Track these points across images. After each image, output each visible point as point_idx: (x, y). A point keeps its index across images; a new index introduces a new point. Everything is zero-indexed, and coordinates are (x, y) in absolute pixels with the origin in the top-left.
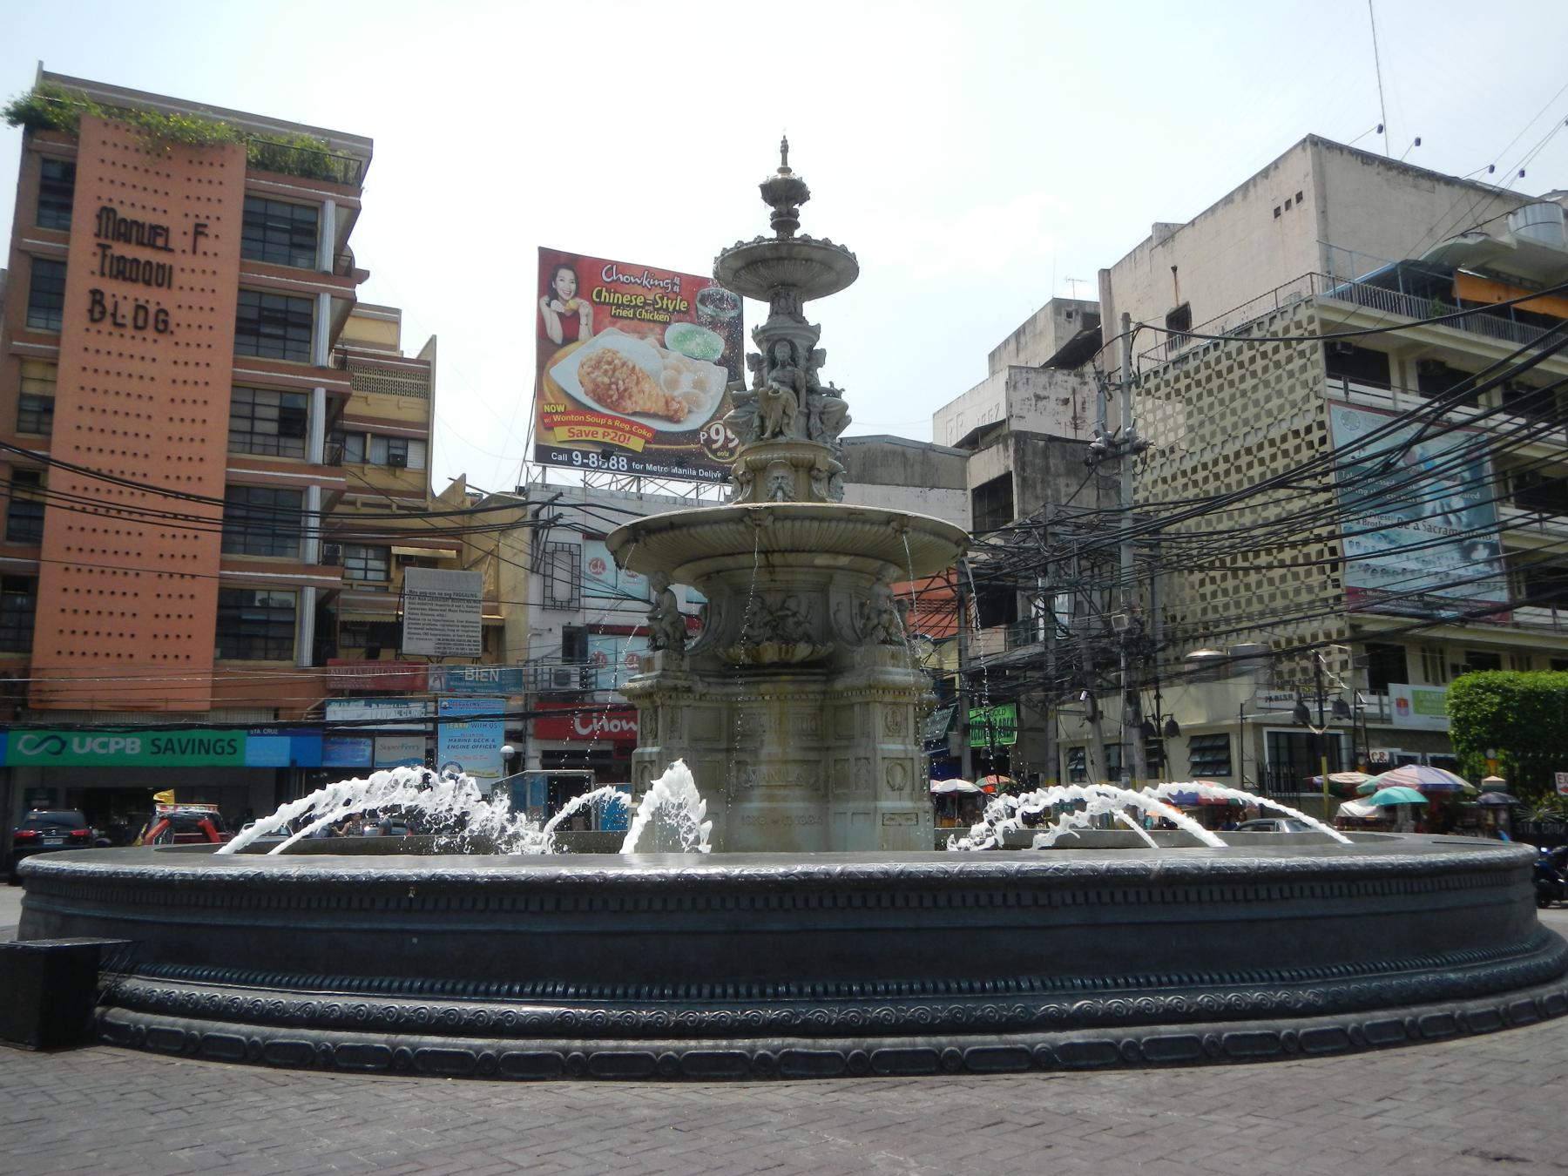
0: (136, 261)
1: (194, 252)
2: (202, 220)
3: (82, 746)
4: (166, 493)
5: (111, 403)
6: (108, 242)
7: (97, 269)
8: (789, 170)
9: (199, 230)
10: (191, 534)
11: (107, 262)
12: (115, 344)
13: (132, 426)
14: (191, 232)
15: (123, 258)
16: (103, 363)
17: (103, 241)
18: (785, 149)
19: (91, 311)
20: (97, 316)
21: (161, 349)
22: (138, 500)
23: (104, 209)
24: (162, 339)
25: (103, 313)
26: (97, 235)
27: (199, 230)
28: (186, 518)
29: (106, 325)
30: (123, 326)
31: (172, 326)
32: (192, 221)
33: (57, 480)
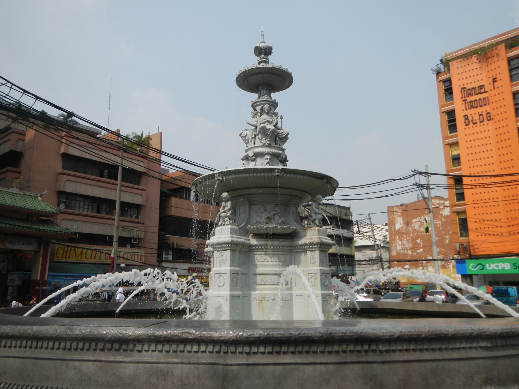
0: (476, 100)
1: (494, 89)
2: (494, 77)
3: (490, 267)
4: (502, 175)
5: (477, 149)
6: (466, 98)
7: (464, 109)
9: (495, 80)
10: (514, 187)
11: (467, 105)
12: (475, 130)
13: (486, 155)
14: (492, 82)
15: (471, 101)
16: (472, 137)
17: (464, 99)
19: (465, 122)
20: (467, 123)
21: (489, 126)
22: (493, 180)
23: (462, 88)
24: (490, 122)
25: (469, 122)
26: (462, 98)
27: (495, 80)
28: (511, 182)
29: (471, 124)
30: (476, 123)
31: (492, 117)
32: (491, 78)
33: (466, 180)
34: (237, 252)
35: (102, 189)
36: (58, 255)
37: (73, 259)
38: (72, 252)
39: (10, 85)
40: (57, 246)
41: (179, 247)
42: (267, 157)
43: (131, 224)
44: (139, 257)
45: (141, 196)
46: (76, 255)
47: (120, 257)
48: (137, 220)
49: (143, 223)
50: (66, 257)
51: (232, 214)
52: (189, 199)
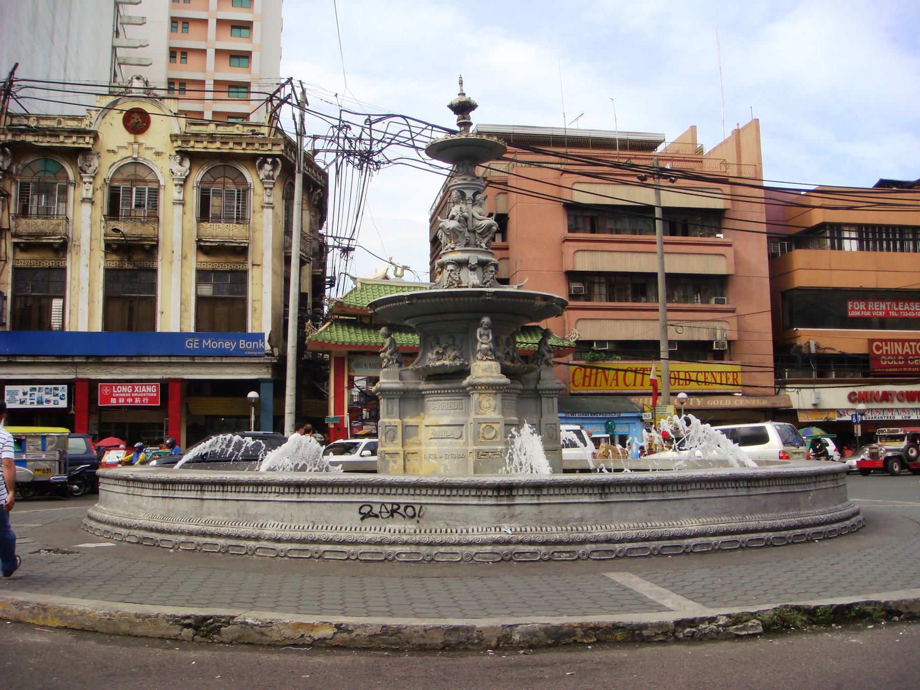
8: (464, 94)
18: (461, 83)
34: (397, 401)
35: (643, 255)
36: (576, 383)
37: (605, 389)
38: (599, 375)
39: (430, 128)
40: (572, 368)
41: (821, 351)
42: (450, 267)
43: (707, 316)
44: (730, 376)
45: (723, 258)
46: (606, 380)
47: (690, 380)
48: (719, 306)
49: (733, 311)
50: (589, 385)
51: (391, 354)
52: (840, 247)
